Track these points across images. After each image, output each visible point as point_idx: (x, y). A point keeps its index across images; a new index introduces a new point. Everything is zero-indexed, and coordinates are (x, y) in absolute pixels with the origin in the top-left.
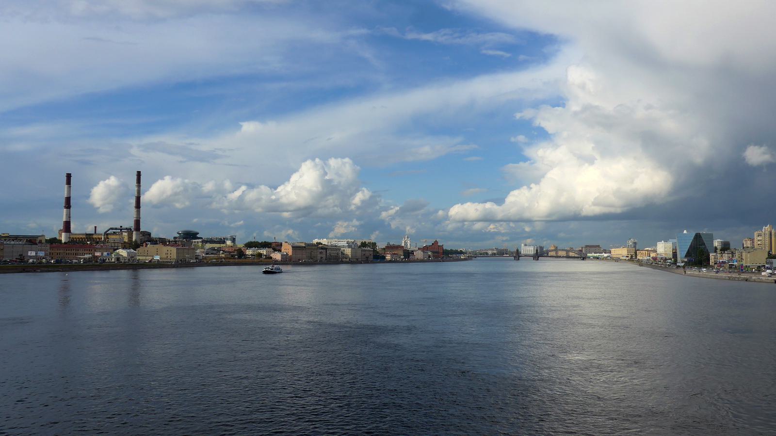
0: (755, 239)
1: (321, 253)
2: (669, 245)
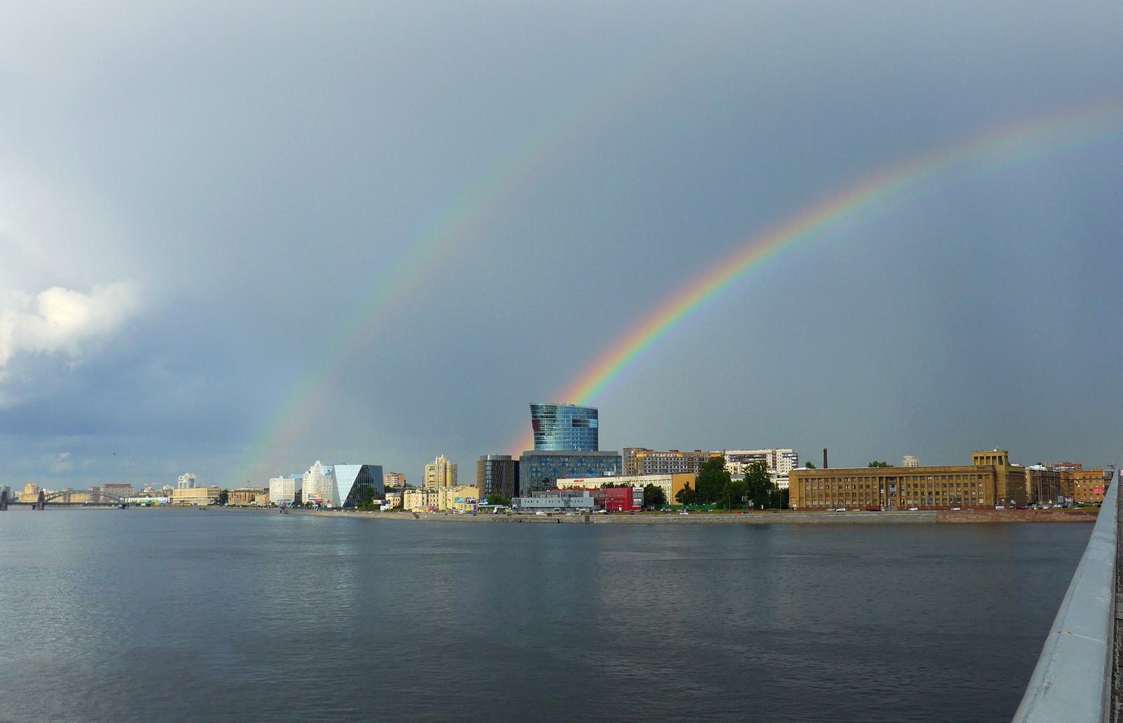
0: (426, 473)
2: (291, 482)
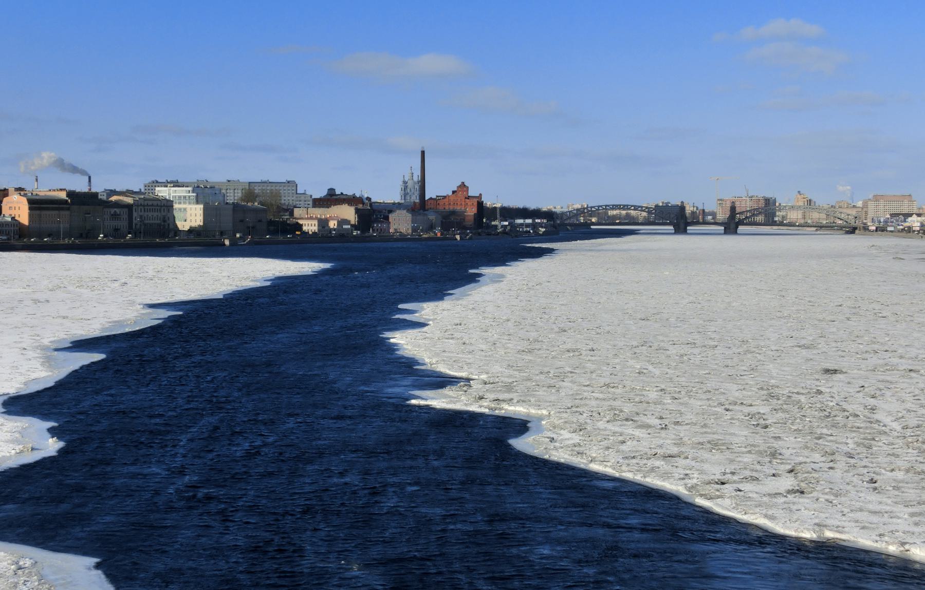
1: (115, 216)
